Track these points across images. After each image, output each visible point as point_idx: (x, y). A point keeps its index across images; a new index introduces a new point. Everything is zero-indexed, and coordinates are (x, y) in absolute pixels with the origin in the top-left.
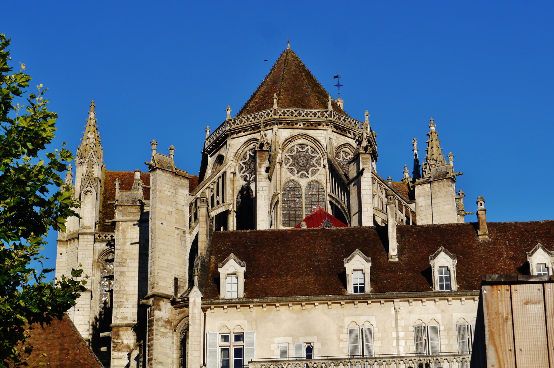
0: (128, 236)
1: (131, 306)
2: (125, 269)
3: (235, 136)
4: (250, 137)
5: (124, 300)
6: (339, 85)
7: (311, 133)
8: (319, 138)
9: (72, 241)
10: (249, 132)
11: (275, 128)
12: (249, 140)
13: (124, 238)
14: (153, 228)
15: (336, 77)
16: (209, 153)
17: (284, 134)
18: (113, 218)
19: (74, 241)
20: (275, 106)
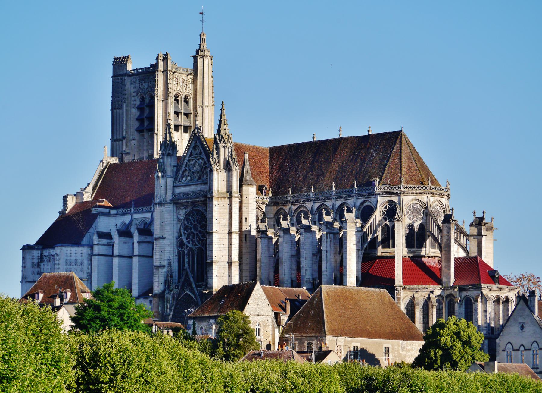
0: (352, 239)
1: (353, 277)
2: (351, 257)
3: (406, 194)
4: (414, 197)
5: (351, 273)
6: (203, 21)
7: (440, 199)
8: (443, 202)
9: (223, 198)
10: (414, 195)
11: (429, 196)
12: (414, 199)
13: (350, 240)
14: (398, 251)
15: (201, 14)
16: (379, 194)
17: (432, 199)
18: (346, 229)
20: (430, 184)
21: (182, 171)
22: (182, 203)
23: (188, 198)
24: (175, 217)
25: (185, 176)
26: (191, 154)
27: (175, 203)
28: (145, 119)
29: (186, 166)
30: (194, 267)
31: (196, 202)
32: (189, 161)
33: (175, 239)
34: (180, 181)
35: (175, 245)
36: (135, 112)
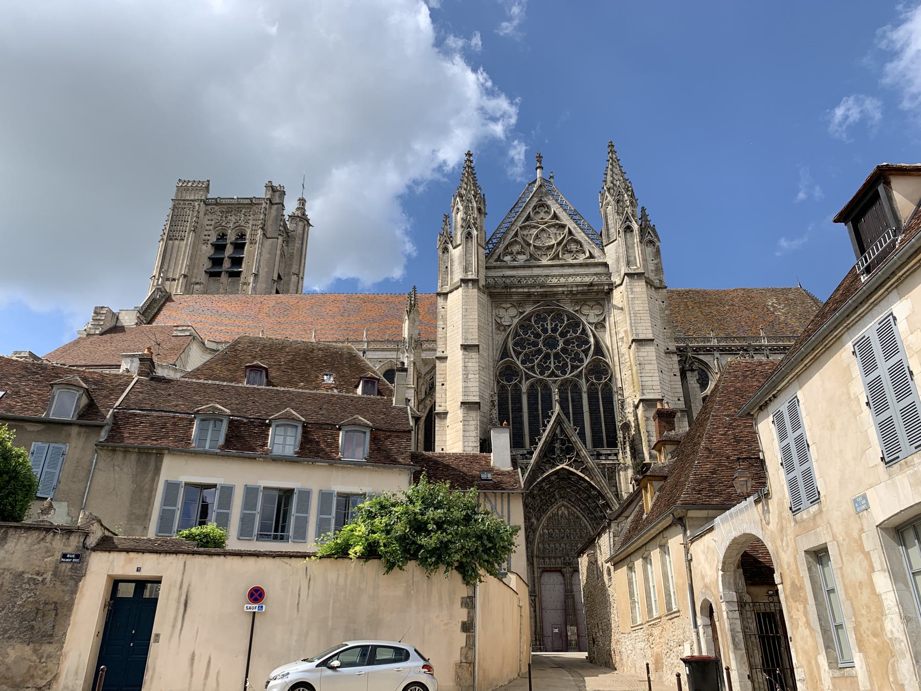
19: (651, 288)
21: (506, 242)
22: (511, 294)
23: (534, 287)
24: (490, 320)
25: (511, 253)
26: (528, 218)
27: (492, 295)
28: (226, 258)
29: (516, 235)
30: (522, 423)
31: (556, 294)
32: (521, 228)
33: (491, 360)
34: (498, 259)
35: (492, 373)
36: (207, 250)
